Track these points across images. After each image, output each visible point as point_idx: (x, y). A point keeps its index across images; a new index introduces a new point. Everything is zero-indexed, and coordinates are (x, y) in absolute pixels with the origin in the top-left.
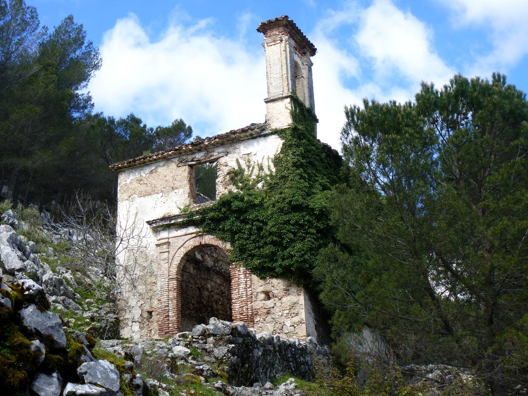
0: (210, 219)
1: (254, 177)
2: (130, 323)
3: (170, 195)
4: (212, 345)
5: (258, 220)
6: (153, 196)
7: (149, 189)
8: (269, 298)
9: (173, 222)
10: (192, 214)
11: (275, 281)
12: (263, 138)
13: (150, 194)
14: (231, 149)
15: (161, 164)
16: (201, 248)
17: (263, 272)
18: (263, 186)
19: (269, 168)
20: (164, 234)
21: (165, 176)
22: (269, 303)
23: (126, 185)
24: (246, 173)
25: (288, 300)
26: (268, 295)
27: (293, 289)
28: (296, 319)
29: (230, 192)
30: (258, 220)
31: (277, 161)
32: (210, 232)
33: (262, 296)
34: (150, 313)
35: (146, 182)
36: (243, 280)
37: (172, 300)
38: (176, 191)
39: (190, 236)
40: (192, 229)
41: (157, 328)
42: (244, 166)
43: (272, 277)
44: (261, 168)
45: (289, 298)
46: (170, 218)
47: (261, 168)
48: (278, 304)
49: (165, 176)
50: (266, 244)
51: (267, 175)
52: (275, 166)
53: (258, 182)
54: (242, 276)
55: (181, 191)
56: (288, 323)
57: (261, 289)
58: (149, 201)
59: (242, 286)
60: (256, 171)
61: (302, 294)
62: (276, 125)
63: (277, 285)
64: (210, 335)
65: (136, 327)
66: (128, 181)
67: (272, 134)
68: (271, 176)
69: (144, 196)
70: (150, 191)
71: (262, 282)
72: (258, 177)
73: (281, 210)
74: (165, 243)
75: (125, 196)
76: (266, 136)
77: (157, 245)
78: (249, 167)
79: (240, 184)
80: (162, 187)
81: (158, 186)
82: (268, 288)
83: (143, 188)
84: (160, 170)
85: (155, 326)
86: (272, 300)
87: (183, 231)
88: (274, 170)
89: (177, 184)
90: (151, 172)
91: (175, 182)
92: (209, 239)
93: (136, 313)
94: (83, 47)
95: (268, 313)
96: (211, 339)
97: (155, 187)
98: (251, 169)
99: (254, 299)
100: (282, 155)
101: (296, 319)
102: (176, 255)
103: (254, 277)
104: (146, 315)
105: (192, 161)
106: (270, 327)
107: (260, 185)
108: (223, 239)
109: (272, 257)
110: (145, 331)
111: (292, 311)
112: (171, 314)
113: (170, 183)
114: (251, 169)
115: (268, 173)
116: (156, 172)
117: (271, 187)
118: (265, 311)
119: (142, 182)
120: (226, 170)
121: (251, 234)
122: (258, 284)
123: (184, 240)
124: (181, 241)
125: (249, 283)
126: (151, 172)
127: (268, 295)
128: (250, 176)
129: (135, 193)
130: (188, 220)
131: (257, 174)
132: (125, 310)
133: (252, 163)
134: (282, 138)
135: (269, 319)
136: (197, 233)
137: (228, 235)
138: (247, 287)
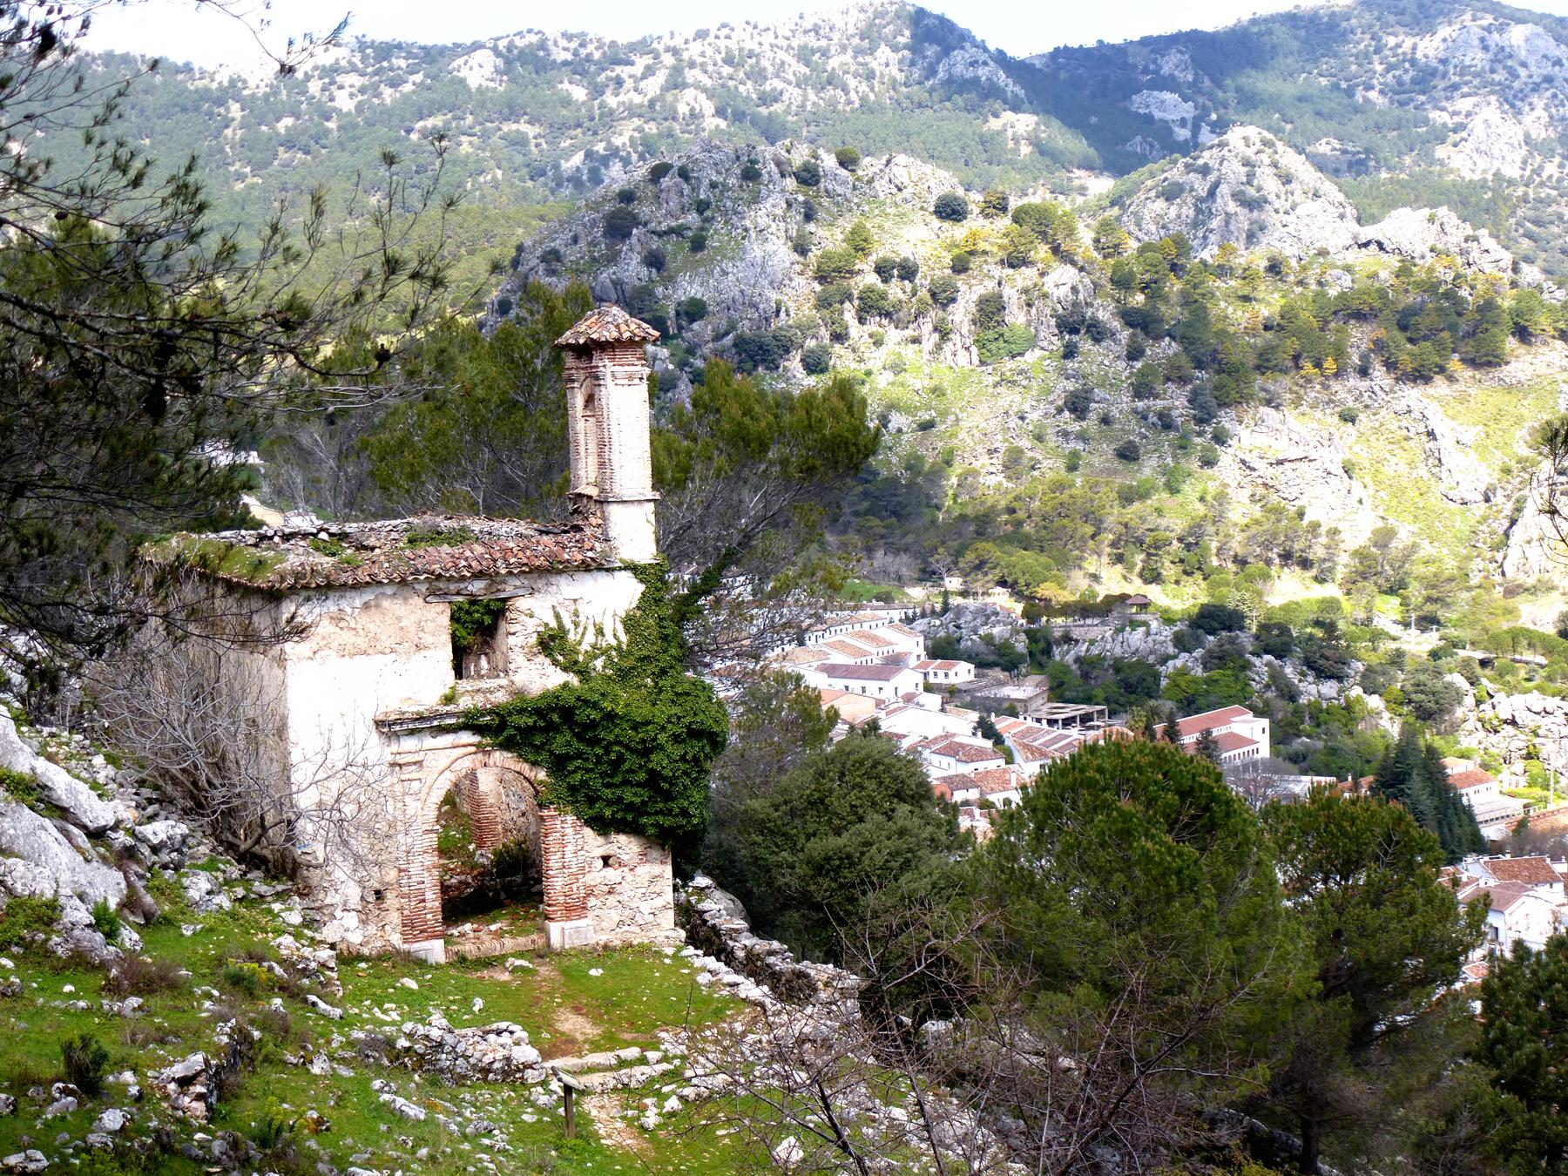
0: (518, 728)
1: (585, 646)
2: (338, 913)
5: (620, 743)
7: (362, 642)
9: (436, 723)
11: (622, 838)
12: (604, 574)
14: (540, 584)
15: (389, 591)
17: (602, 826)
18: (604, 667)
19: (614, 634)
20: (409, 743)
21: (399, 619)
22: (612, 874)
24: (571, 636)
25: (646, 871)
27: (655, 853)
28: (659, 902)
30: (620, 743)
31: (630, 623)
32: (507, 745)
34: (379, 894)
35: (353, 625)
37: (428, 870)
38: (424, 653)
40: (467, 737)
41: (399, 921)
42: (568, 625)
43: (618, 832)
44: (600, 632)
47: (600, 632)
48: (629, 877)
49: (399, 619)
50: (626, 783)
51: (612, 647)
52: (627, 631)
53: (596, 657)
54: (570, 831)
56: (646, 907)
57: (601, 852)
59: (570, 849)
60: (590, 637)
61: (669, 861)
63: (626, 846)
65: (352, 920)
67: (620, 569)
68: (618, 649)
69: (352, 655)
70: (364, 646)
71: (601, 840)
72: (594, 647)
73: (676, 739)
76: (610, 570)
77: (393, 765)
78: (576, 625)
79: (560, 658)
80: (392, 640)
81: (384, 638)
83: (347, 637)
84: (386, 603)
85: (394, 917)
87: (448, 739)
88: (624, 638)
89: (428, 639)
90: (366, 606)
91: (421, 635)
93: (353, 893)
98: (580, 630)
100: (638, 613)
102: (437, 785)
103: (588, 831)
104: (372, 898)
105: (458, 594)
107: (599, 663)
108: (534, 764)
109: (640, 810)
110: (372, 929)
111: (652, 889)
112: (429, 895)
113: (411, 635)
114: (580, 630)
115: (614, 643)
116: (378, 606)
117: (623, 675)
118: (606, 889)
119: (343, 624)
120: (532, 625)
121: (597, 763)
122: (594, 843)
124: (444, 759)
125: (580, 842)
126: (366, 606)
128: (580, 643)
129: (328, 646)
131: (593, 640)
133: (582, 618)
134: (641, 581)
135: (612, 900)
136: (478, 745)
137: (544, 755)
138: (574, 850)
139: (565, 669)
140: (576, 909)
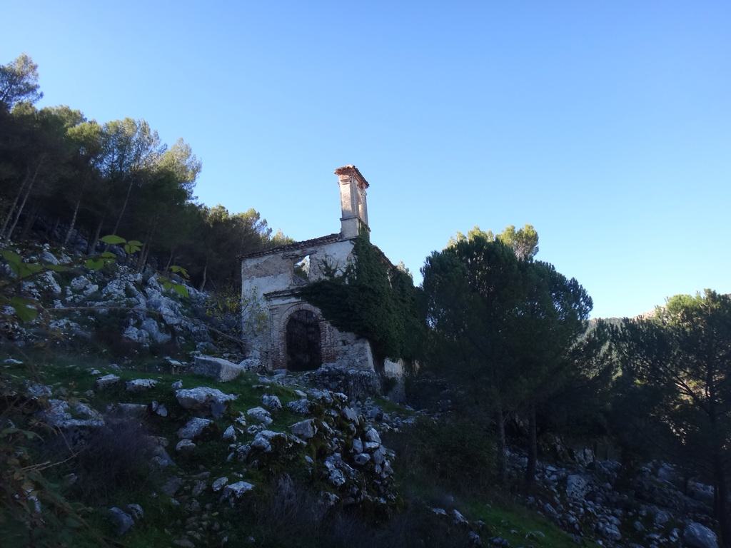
3: (278, 277)
4: (328, 381)
6: (267, 277)
7: (263, 273)
8: (345, 345)
10: (292, 291)
11: (349, 334)
13: (265, 276)
14: (318, 249)
16: (299, 312)
22: (345, 348)
23: (247, 269)
25: (357, 346)
26: (344, 343)
29: (320, 279)
33: (341, 343)
36: (328, 333)
39: (291, 304)
40: (293, 300)
45: (358, 345)
46: (280, 292)
55: (286, 274)
58: (262, 281)
62: (348, 235)
63: (350, 336)
64: (326, 375)
66: (249, 267)
69: (260, 277)
74: (276, 309)
75: (247, 276)
82: (344, 338)
83: (259, 271)
86: (347, 346)
87: (288, 301)
89: (283, 270)
92: (307, 306)
94: (191, 157)
95: (345, 354)
96: (327, 377)
97: (268, 271)
99: (335, 345)
101: (362, 358)
104: (264, 355)
106: (346, 362)
112: (281, 353)
123: (287, 306)
127: (344, 343)
130: (291, 293)
132: (249, 351)
135: (345, 357)
138: (331, 336)
139: (325, 275)
140: (333, 359)
